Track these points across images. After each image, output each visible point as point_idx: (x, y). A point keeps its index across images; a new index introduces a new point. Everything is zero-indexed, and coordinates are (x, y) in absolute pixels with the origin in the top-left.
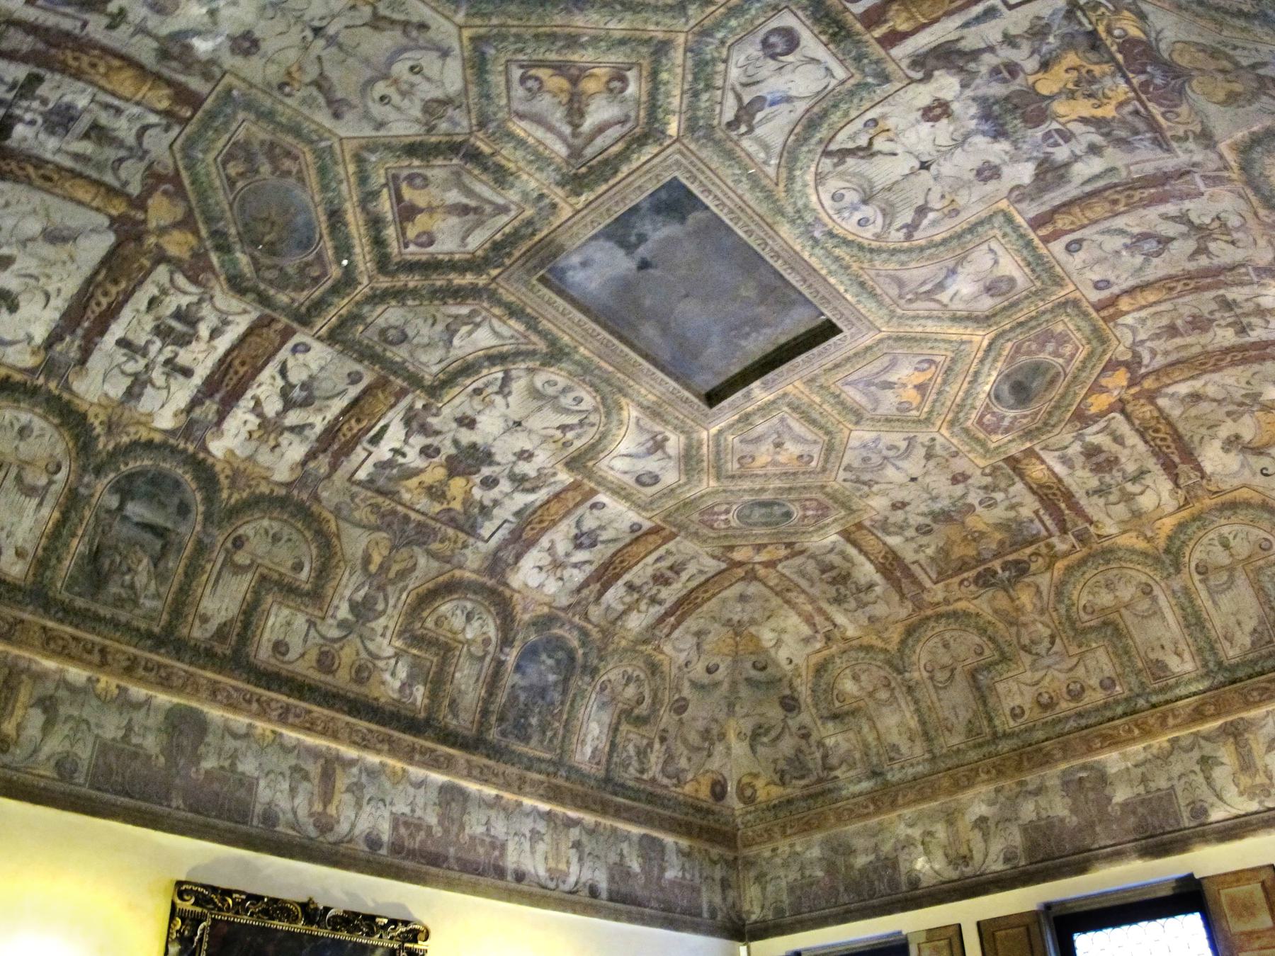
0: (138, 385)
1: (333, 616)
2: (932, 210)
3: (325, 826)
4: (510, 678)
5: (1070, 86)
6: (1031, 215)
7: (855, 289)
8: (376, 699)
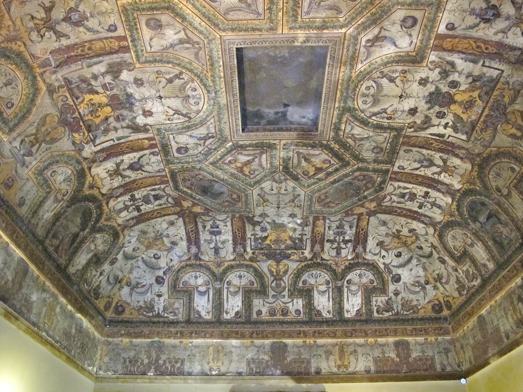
2: (167, 79)
5: (99, 109)
6: (128, 55)
7: (216, 65)
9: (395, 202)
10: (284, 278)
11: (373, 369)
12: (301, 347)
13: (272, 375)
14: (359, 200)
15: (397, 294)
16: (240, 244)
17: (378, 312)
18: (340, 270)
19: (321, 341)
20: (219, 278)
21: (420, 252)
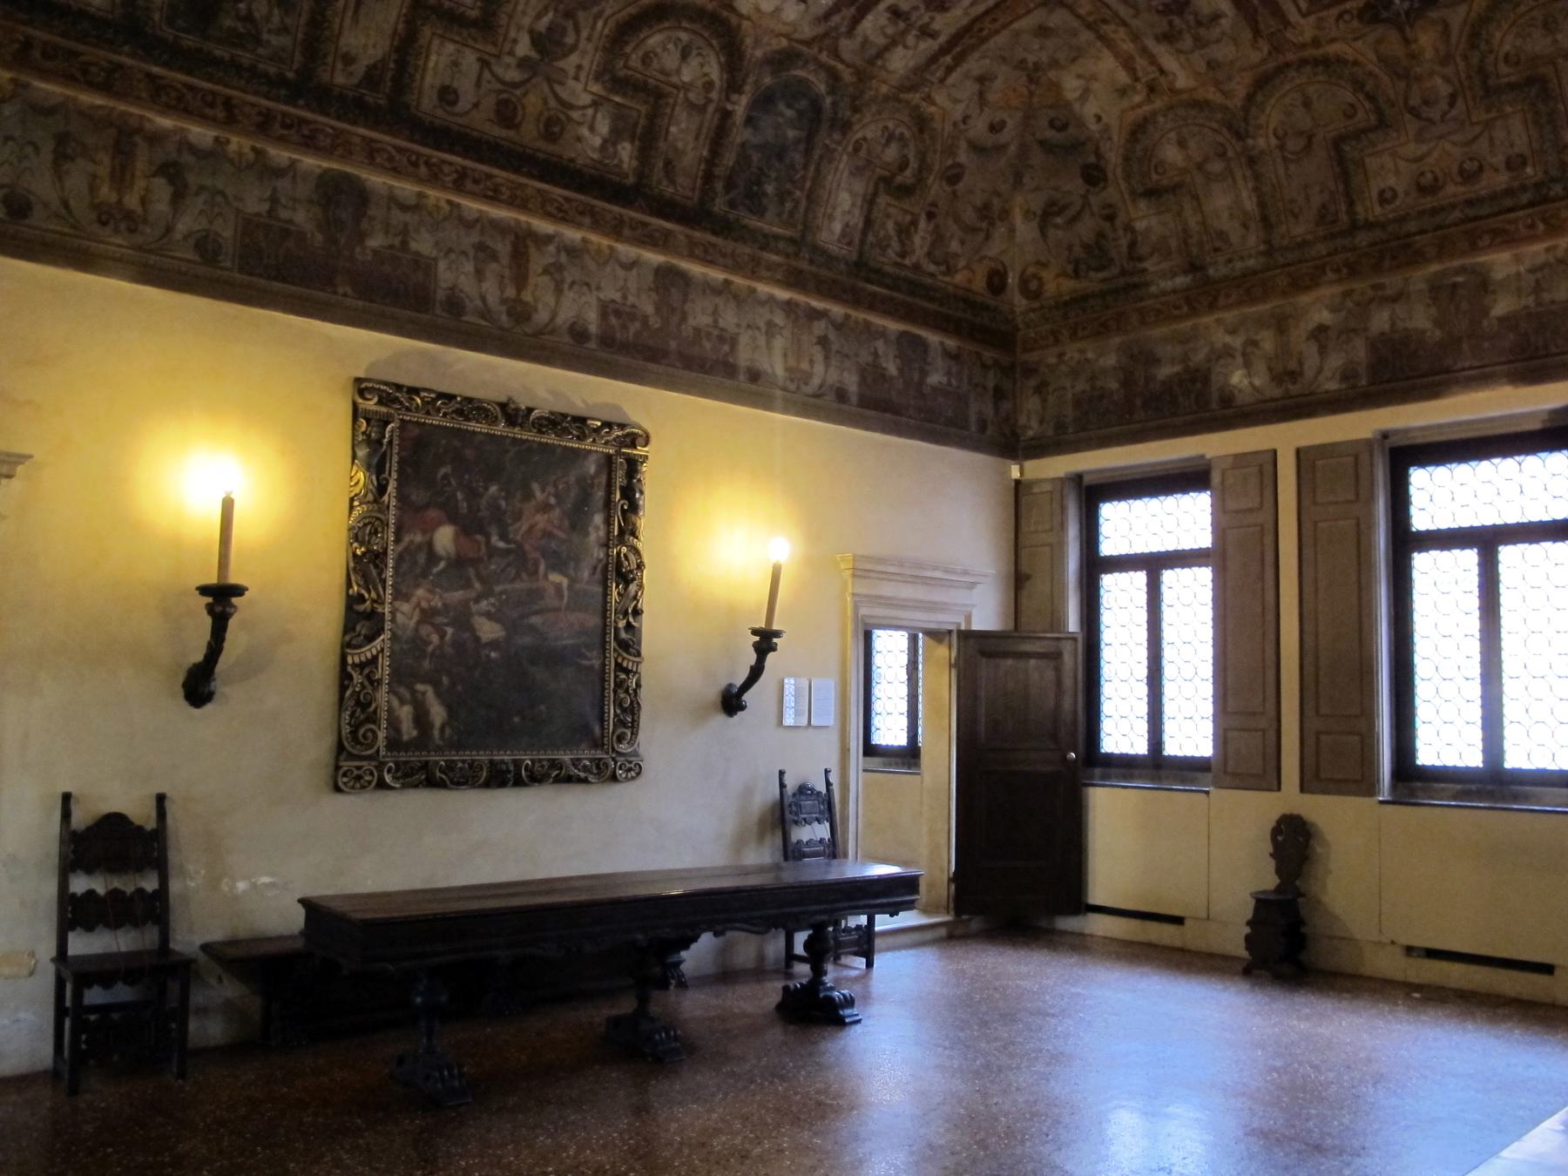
1: (511, 53)
3: (520, 312)
4: (740, 135)
8: (572, 160)
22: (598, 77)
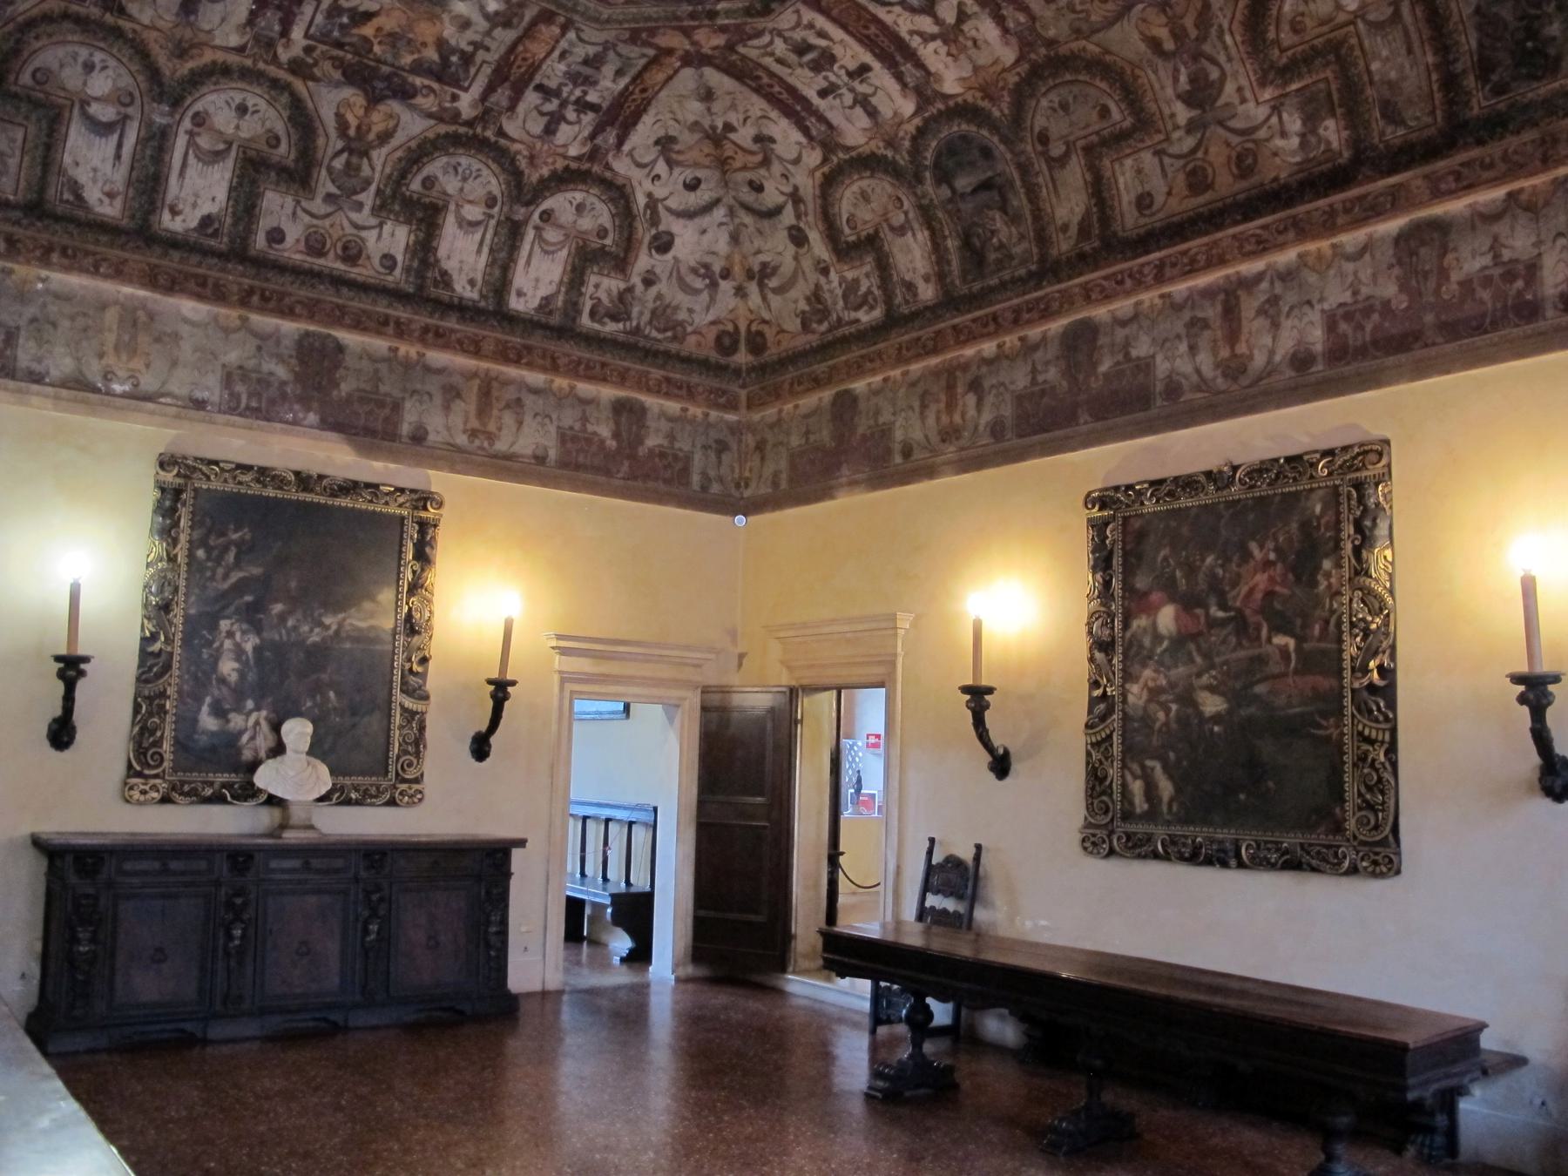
0: (863, 102)
1: (1177, 127)
8: (1276, 179)
9: (772, 54)
10: (374, 154)
11: (553, 454)
12: (384, 360)
13: (295, 423)
14: (692, 16)
15: (649, 282)
16: (279, 8)
17: (593, 314)
18: (535, 178)
19: (437, 357)
20: (174, 95)
21: (748, 197)
22: (1263, 83)
